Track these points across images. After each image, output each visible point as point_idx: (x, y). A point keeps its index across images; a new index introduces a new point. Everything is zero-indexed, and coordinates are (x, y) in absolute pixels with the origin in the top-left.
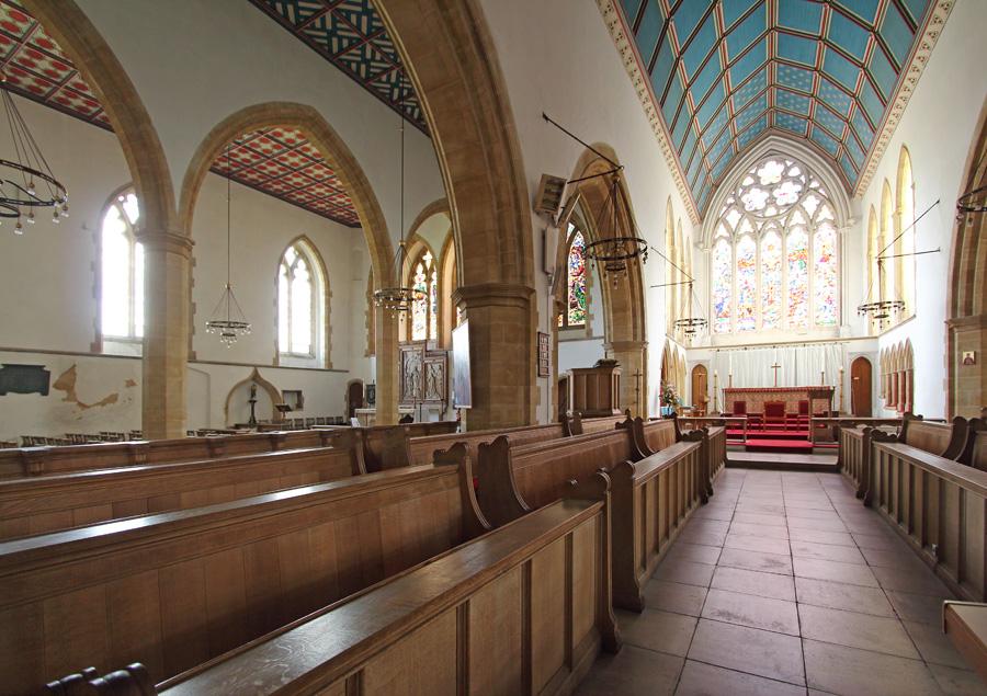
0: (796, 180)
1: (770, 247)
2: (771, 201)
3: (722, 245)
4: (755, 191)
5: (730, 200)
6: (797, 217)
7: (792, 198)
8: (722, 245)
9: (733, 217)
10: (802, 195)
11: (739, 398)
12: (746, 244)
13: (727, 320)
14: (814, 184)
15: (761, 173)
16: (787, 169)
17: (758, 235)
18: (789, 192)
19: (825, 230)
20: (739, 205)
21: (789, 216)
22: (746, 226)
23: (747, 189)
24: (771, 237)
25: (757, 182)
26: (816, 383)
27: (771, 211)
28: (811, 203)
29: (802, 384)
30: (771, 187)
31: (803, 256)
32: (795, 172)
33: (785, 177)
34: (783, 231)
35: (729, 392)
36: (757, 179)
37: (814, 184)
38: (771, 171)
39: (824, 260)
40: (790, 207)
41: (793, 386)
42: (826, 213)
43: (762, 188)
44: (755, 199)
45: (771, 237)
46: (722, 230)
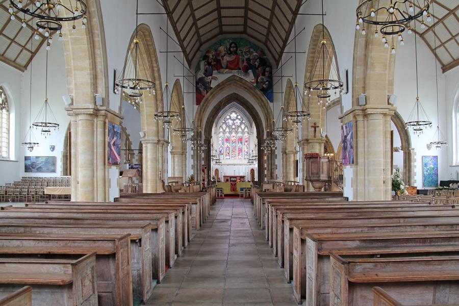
0: (239, 119)
1: (234, 137)
2: (234, 124)
3: (221, 134)
4: (230, 120)
5: (223, 122)
6: (240, 130)
7: (239, 124)
8: (221, 134)
9: (224, 126)
10: (241, 123)
11: (227, 178)
12: (228, 135)
13: (222, 156)
14: (244, 122)
15: (231, 115)
16: (237, 116)
17: (230, 133)
18: (238, 122)
19: (246, 134)
20: (225, 123)
21: (238, 129)
22: (227, 130)
23: (228, 119)
24: (234, 134)
25: (230, 118)
26: (242, 175)
27: (234, 127)
28: (243, 126)
29: (240, 175)
30: (234, 120)
31: (241, 140)
32: (239, 117)
33: (237, 118)
34: (237, 132)
35: (224, 177)
36: (230, 117)
37: (244, 122)
38: (234, 115)
39: (246, 142)
40: (239, 127)
41: (238, 175)
42: (246, 130)
43: (231, 120)
44: (230, 122)
45: (234, 134)
46: (221, 130)
